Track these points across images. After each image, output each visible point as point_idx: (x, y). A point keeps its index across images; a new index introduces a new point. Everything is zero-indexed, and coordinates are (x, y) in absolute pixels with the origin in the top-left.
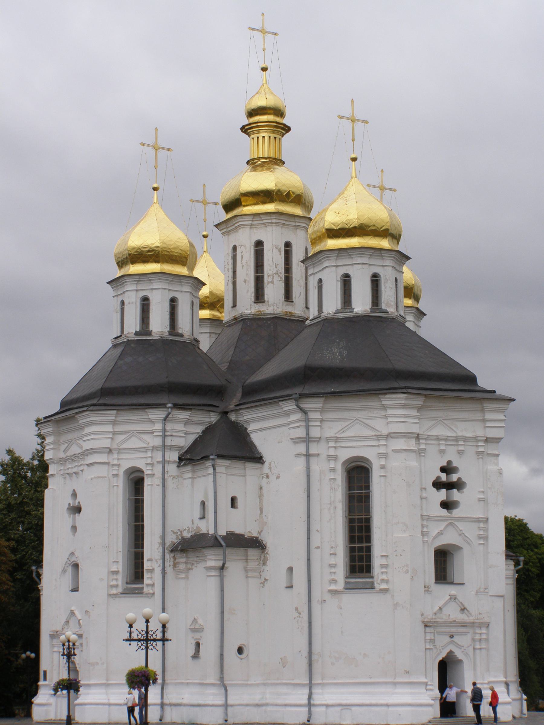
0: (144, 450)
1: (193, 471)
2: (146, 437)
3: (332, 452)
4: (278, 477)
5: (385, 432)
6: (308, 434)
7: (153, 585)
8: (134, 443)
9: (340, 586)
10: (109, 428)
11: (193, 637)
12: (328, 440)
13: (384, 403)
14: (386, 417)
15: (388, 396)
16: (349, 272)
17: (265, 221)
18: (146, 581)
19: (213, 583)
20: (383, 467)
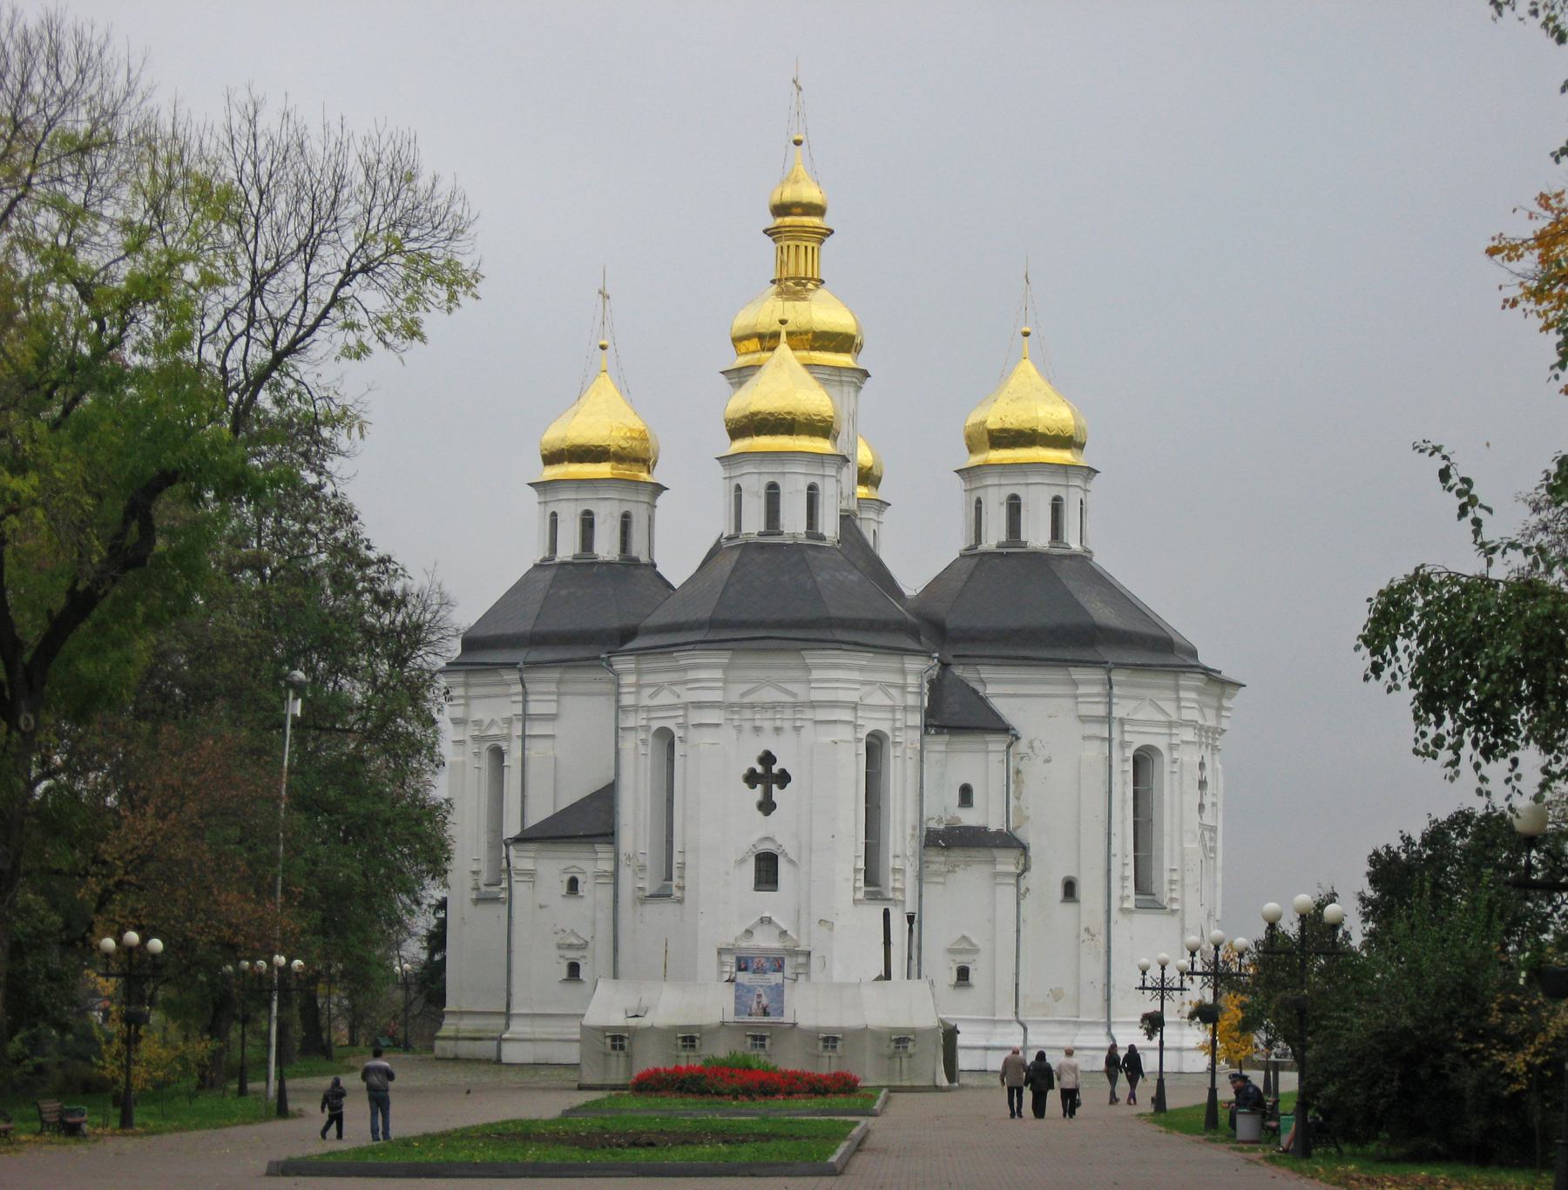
0: (893, 709)
1: (948, 744)
2: (893, 691)
3: (1127, 737)
4: (1048, 761)
5: (1174, 717)
6: (1110, 713)
7: (903, 890)
8: (878, 698)
9: (1130, 904)
10: (856, 675)
11: (954, 960)
12: (1122, 721)
13: (1181, 682)
14: (1178, 700)
15: (1187, 675)
16: (1062, 493)
17: (844, 379)
18: (891, 885)
19: (1007, 893)
20: (1174, 761)
